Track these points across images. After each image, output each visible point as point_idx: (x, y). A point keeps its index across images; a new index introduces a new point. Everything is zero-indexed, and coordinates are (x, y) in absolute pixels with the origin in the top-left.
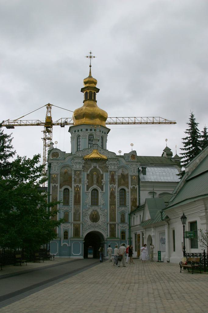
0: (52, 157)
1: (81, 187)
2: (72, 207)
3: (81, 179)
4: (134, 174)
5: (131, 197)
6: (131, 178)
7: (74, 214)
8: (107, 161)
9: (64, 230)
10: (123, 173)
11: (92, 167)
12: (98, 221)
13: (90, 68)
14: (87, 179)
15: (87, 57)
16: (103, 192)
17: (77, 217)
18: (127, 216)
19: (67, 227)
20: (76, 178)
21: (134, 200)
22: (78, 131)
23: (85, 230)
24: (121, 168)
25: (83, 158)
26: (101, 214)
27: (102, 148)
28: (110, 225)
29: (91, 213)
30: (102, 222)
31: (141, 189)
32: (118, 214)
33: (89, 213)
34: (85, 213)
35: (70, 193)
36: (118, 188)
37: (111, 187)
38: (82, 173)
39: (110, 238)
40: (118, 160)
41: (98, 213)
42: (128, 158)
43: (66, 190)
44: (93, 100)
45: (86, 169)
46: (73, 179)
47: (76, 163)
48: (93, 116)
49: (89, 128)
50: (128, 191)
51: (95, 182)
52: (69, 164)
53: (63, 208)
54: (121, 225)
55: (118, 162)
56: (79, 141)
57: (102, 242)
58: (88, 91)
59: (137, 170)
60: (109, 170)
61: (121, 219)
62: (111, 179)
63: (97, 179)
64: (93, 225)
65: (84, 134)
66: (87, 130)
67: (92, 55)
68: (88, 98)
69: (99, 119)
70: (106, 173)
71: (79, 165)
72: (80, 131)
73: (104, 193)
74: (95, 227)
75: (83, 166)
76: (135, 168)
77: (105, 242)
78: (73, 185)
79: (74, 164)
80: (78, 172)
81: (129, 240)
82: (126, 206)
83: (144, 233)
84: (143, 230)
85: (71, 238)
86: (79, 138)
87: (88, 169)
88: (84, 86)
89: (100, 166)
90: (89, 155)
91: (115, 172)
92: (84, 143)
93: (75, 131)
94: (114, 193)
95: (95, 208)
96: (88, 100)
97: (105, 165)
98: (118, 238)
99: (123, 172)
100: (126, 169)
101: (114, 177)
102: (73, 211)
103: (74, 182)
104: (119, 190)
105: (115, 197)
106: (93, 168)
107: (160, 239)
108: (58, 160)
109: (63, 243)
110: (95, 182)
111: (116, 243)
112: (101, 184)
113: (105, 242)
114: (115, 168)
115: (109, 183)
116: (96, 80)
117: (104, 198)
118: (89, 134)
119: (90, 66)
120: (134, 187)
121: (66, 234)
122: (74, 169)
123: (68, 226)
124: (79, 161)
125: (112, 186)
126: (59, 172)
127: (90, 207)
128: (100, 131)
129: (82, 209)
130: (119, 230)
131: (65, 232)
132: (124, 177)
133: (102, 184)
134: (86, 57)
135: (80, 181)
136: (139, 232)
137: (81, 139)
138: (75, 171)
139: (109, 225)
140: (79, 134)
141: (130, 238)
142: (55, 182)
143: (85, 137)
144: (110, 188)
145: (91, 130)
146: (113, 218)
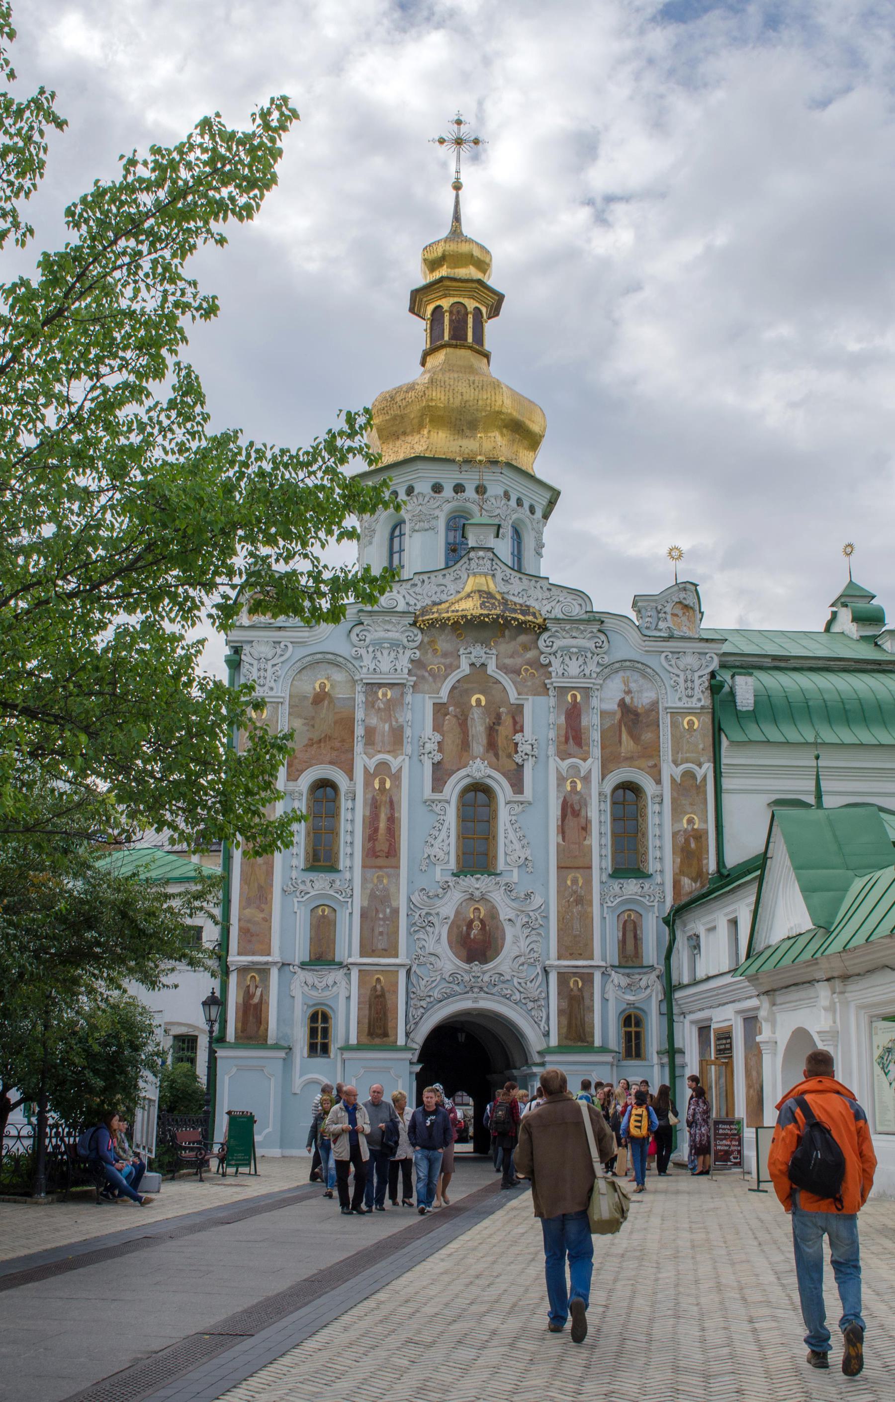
3: (401, 729)
4: (689, 705)
5: (678, 827)
6: (675, 725)
7: (364, 915)
8: (545, 635)
9: (309, 1006)
10: (628, 700)
13: (457, 196)
14: (437, 728)
15: (442, 141)
16: (519, 798)
17: (381, 933)
18: (652, 932)
20: (374, 721)
21: (693, 845)
23: (423, 1003)
25: (411, 620)
26: (512, 915)
27: (519, 571)
28: (563, 978)
29: (457, 913)
30: (522, 959)
31: (726, 783)
33: (448, 907)
34: (424, 913)
35: (344, 804)
37: (565, 774)
38: (408, 698)
39: (561, 1049)
40: (600, 631)
41: (493, 914)
42: (659, 619)
45: (430, 679)
46: (359, 731)
47: (378, 645)
48: (463, 421)
49: (448, 478)
50: (660, 795)
51: (478, 746)
53: (302, 887)
55: (603, 637)
56: (396, 548)
57: (515, 1072)
58: (446, 303)
59: (707, 684)
60: (556, 680)
61: (623, 942)
62: (563, 732)
63: (492, 731)
64: (466, 978)
65: (423, 509)
66: (437, 488)
68: (446, 338)
69: (502, 435)
71: (393, 654)
74: (481, 988)
75: (412, 661)
77: (535, 1069)
78: (362, 761)
79: (363, 651)
80: (385, 695)
81: (666, 1060)
82: (649, 876)
83: (762, 1014)
84: (754, 1002)
85: (347, 1048)
86: (397, 533)
87: (438, 677)
88: (420, 277)
89: (508, 661)
90: (447, 605)
91: (586, 691)
97: (530, 655)
98: (604, 1050)
99: (628, 692)
100: (644, 675)
101: (579, 715)
102: (358, 902)
104: (608, 788)
105: (585, 829)
106: (467, 671)
107: (877, 1053)
109: (301, 1076)
112: (510, 756)
114: (587, 672)
115: (552, 750)
116: (488, 252)
117: (526, 832)
118: (447, 507)
119: (457, 187)
120: (689, 775)
121: (320, 1025)
122: (364, 675)
123: (330, 983)
124: (390, 635)
127: (452, 880)
128: (507, 495)
131: (314, 1018)
132: (633, 719)
133: (520, 761)
135: (397, 738)
136: (725, 1017)
137: (407, 536)
138: (372, 687)
139: (553, 978)
141: (672, 1052)
143: (426, 526)
144: (561, 780)
145: (459, 488)
146: (575, 942)
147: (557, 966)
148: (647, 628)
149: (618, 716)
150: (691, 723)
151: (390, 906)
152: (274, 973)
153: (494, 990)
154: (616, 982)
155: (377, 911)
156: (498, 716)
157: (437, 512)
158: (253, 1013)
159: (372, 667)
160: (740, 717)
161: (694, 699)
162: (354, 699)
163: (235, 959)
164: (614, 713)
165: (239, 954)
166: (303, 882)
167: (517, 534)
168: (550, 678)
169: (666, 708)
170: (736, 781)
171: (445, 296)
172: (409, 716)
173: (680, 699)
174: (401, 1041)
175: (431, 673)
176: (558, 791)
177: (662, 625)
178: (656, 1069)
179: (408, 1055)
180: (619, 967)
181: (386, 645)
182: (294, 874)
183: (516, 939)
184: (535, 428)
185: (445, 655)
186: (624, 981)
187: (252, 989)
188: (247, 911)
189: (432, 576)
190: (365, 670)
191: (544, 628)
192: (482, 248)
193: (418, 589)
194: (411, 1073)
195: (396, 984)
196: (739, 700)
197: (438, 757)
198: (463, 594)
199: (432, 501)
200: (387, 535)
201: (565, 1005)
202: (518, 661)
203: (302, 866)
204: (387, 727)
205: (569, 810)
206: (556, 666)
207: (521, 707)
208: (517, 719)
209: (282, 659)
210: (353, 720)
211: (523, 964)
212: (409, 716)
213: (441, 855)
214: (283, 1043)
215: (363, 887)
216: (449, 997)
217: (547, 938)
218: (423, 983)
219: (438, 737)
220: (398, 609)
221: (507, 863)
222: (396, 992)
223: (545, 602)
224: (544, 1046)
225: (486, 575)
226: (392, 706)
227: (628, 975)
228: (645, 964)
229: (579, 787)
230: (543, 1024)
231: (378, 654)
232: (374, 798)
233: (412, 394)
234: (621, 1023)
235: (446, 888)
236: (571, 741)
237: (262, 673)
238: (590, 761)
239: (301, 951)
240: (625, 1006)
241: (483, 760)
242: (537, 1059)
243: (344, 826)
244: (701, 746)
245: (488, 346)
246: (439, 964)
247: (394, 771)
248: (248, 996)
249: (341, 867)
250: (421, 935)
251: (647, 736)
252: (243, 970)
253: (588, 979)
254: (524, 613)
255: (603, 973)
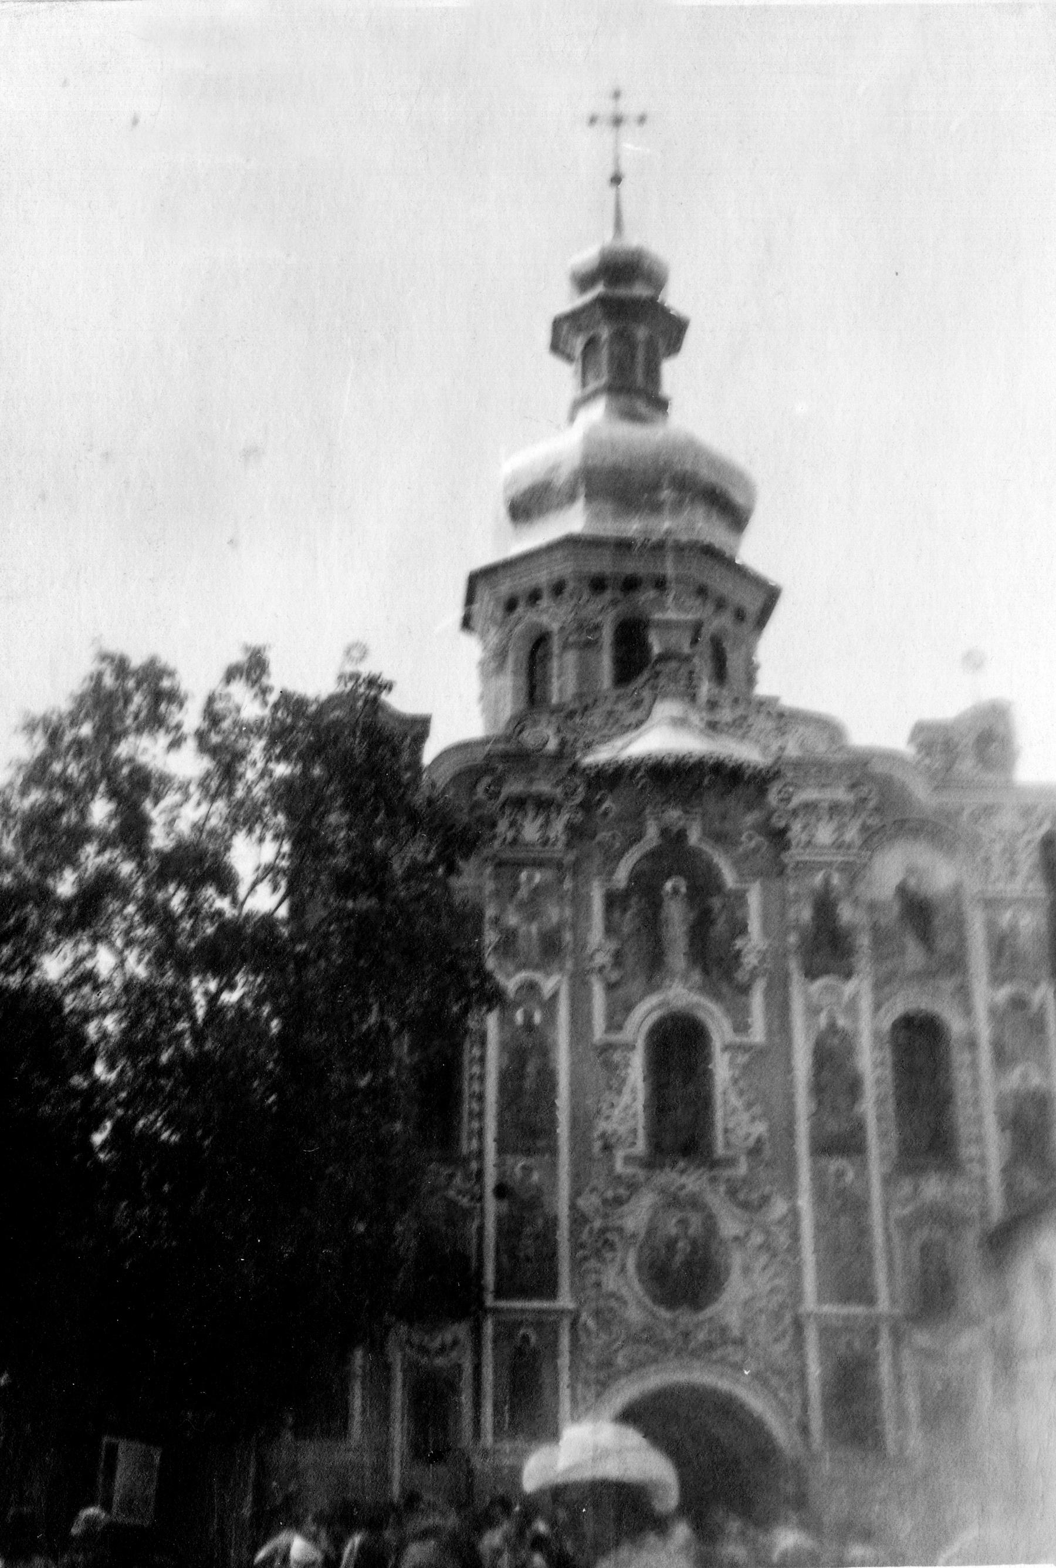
1: (555, 996)
14: (610, 930)
19: (443, 1350)
20: (512, 920)
28: (827, 1332)
47: (519, 803)
51: (677, 958)
64: (668, 1334)
67: (629, 107)
80: (530, 879)
104: (886, 1025)
105: (854, 1088)
110: (677, 958)
115: (794, 965)
119: (616, 180)
127: (641, 1174)
129: (576, 1193)
140: (545, 619)
144: (813, 1011)
147: (818, 1317)
149: (896, 909)
159: (510, 835)
200: (524, 655)
204: (534, 928)
207: (740, 897)
213: (622, 1130)
221: (728, 1145)
235: (633, 1187)
250: (592, 1263)
251: (945, 943)
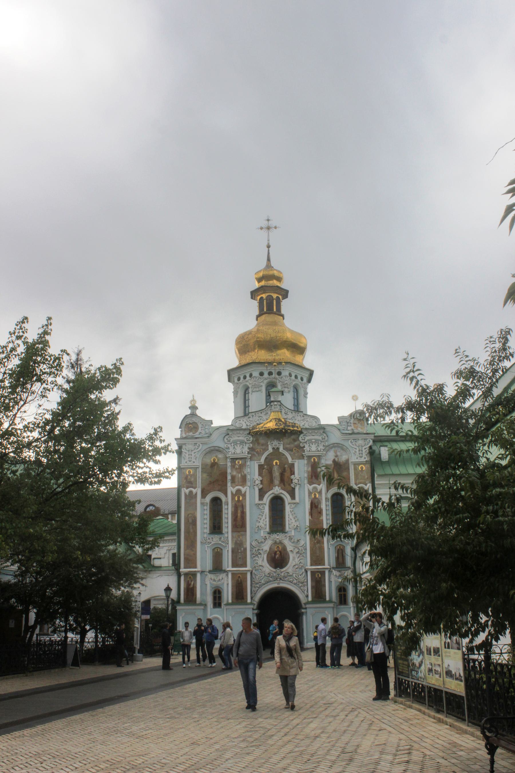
0: (185, 434)
1: (245, 492)
2: (227, 537)
3: (245, 475)
4: (361, 460)
6: (355, 469)
7: (233, 551)
8: (302, 435)
10: (336, 459)
11: (270, 450)
12: (287, 564)
13: (269, 250)
14: (260, 474)
15: (261, 228)
16: (294, 501)
17: (240, 558)
20: (234, 473)
22: (245, 377)
24: (332, 448)
28: (313, 573)
29: (270, 548)
32: (329, 549)
33: (266, 547)
34: (257, 549)
35: (224, 507)
36: (327, 491)
37: (311, 491)
39: (313, 602)
40: (324, 432)
41: (285, 548)
42: (348, 426)
43: (216, 502)
44: (275, 313)
45: (257, 455)
46: (229, 477)
47: (235, 443)
48: (272, 345)
51: (277, 481)
52: (222, 445)
53: (208, 541)
54: (335, 572)
55: (325, 435)
56: (247, 398)
58: (264, 296)
60: (306, 453)
61: (337, 558)
62: (310, 474)
63: (282, 475)
64: (275, 575)
66: (261, 374)
67: (272, 223)
68: (265, 310)
69: (288, 350)
70: (300, 461)
71: (241, 446)
72: (248, 378)
73: (298, 503)
74: (281, 579)
75: (249, 448)
76: (362, 446)
77: (303, 611)
78: (231, 489)
79: (229, 445)
80: (239, 462)
81: (355, 605)
85: (228, 604)
87: (260, 454)
89: (288, 446)
91: (319, 457)
92: (257, 400)
93: (239, 379)
94: (319, 502)
95: (278, 537)
96: (265, 313)
97: (296, 443)
98: (330, 601)
99: (336, 456)
100: (343, 449)
102: (230, 546)
103: (232, 483)
104: (329, 495)
105: (320, 513)
108: (196, 438)
111: (326, 612)
112: (290, 485)
113: (303, 611)
114: (319, 449)
115: (306, 481)
116: (281, 273)
117: (297, 515)
118: (266, 382)
119: (269, 247)
121: (217, 595)
122: (229, 455)
123: (221, 578)
124: (240, 438)
125: (315, 488)
126: (198, 463)
128: (290, 375)
130: (333, 583)
133: (293, 486)
134: (258, 228)
137: (250, 394)
138: (233, 460)
139: (309, 574)
140: (248, 384)
142: (190, 485)
143: (257, 389)
144: (310, 493)
145: (270, 374)
146: (317, 558)
147: (310, 569)
148: (343, 430)
149: (333, 466)
150: (362, 468)
151: (243, 547)
152: (199, 576)
153: (286, 579)
154: (335, 574)
155: (238, 550)
156: (284, 469)
157: (262, 384)
158: (191, 592)
159: (233, 452)
160: (382, 463)
161: (363, 458)
162: (227, 465)
163: (183, 570)
164: (331, 465)
165: (185, 568)
166: (209, 539)
167: (296, 389)
168: (304, 452)
169: (352, 462)
170: (381, 490)
171: (264, 293)
172: (249, 470)
173: (357, 458)
174: (249, 600)
175: (257, 452)
176: (309, 498)
177: (349, 428)
178: (352, 609)
179: (252, 606)
180: (337, 568)
181: (238, 442)
182: (205, 536)
183: (294, 559)
184: (302, 345)
185: (263, 445)
186: (338, 574)
187: (190, 582)
188: (188, 551)
189: (257, 413)
190: (230, 453)
191: (301, 432)
192: (279, 272)
193: (251, 419)
194: (253, 613)
195: (246, 578)
196: (382, 456)
197: (261, 486)
198: (269, 420)
199: (259, 379)
200: (243, 393)
201: (314, 584)
202: (292, 446)
203: (208, 532)
204: (240, 475)
205: (314, 506)
206: (307, 448)
207: (292, 465)
208: (292, 469)
209: (198, 450)
210: (227, 473)
211: (297, 568)
212: (249, 470)
213: (263, 525)
214: (203, 603)
215: (232, 540)
216: (268, 582)
217: (306, 557)
218: (257, 577)
219: (261, 478)
220: (243, 427)
221: (289, 528)
222: (246, 581)
223: (302, 421)
224: (307, 601)
225: (278, 411)
226: (242, 467)
227: (340, 571)
228: (347, 566)
229: (317, 496)
230: (305, 592)
231: (236, 446)
232: (236, 505)
233: (250, 336)
234: (337, 591)
235: (265, 539)
236: (314, 478)
237: (190, 456)
238: (321, 485)
239: (209, 566)
240: (338, 584)
241: (279, 486)
242: (303, 606)
243: (224, 516)
244: (366, 477)
245: (283, 312)
246: (264, 569)
247: (243, 493)
248: (188, 584)
249: (224, 532)
250: (256, 558)
251: (345, 474)
252: (186, 574)
253: (323, 573)
254: (293, 427)
255: (329, 571)
